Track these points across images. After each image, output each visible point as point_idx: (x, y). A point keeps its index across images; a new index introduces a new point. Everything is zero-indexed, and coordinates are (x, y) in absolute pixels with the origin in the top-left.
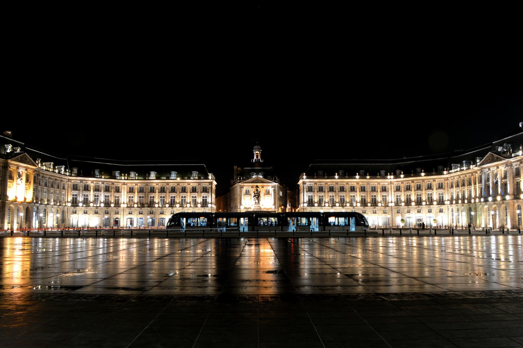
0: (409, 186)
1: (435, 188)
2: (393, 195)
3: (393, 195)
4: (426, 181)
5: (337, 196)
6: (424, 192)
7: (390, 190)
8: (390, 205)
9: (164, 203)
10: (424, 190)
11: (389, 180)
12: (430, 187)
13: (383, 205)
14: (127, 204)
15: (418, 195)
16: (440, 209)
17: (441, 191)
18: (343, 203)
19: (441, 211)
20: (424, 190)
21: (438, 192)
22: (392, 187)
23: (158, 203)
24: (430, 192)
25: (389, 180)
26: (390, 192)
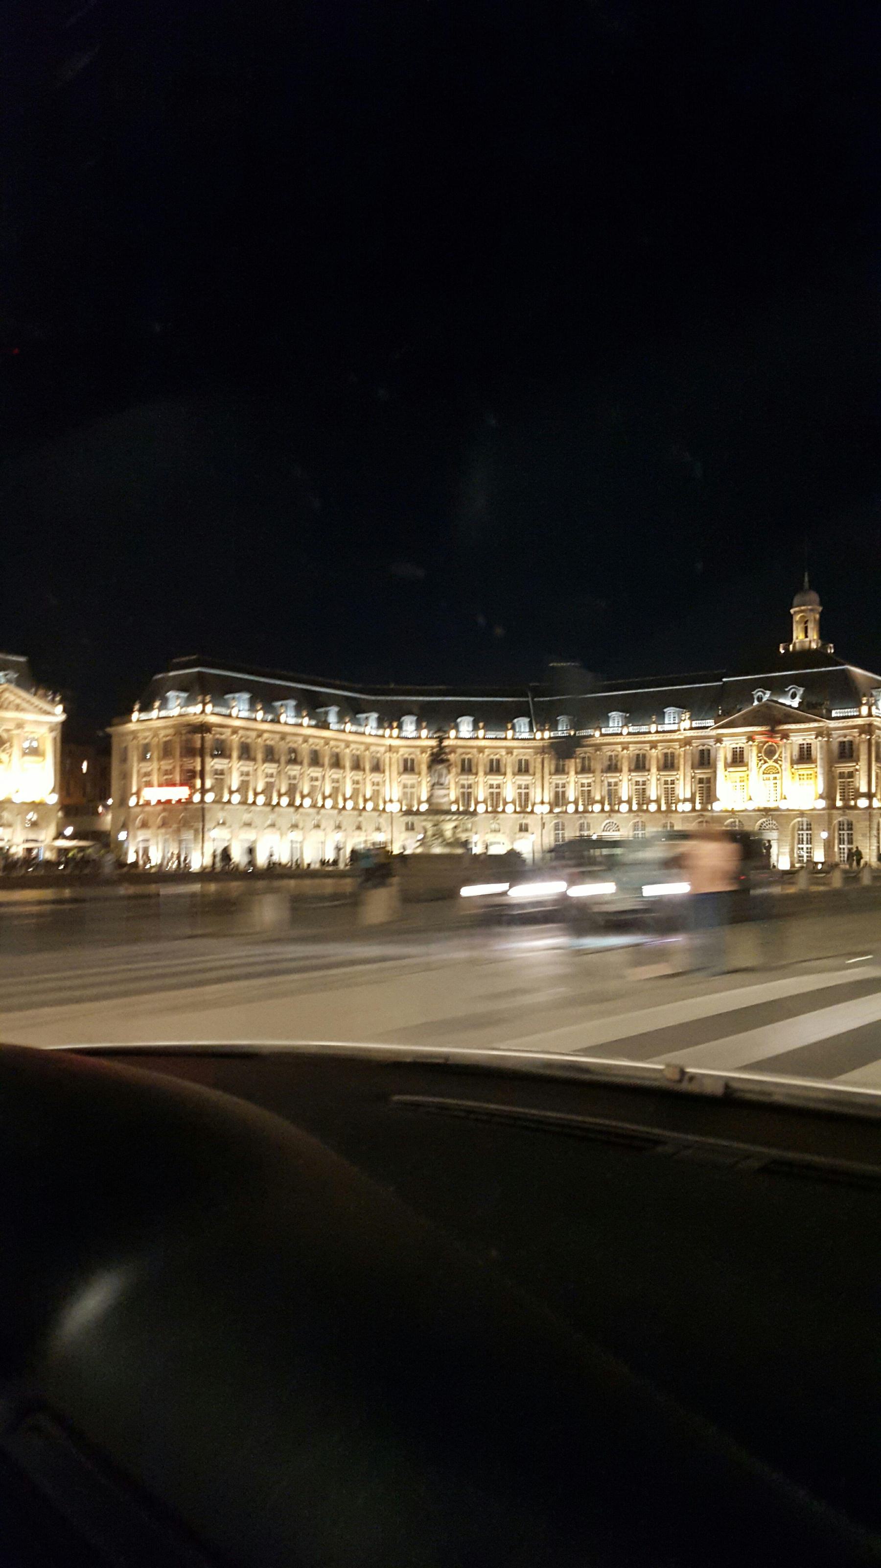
0: (498, 761)
1: (509, 771)
2: (395, 784)
3: (395, 784)
4: (487, 751)
5: (283, 776)
6: (481, 778)
7: (387, 768)
8: (389, 807)
9: (589, 800)
10: (481, 773)
11: (388, 742)
12: (495, 768)
13: (518, 809)
14: (549, 803)
15: (520, 787)
16: (521, 825)
17: (524, 780)
18: (526, 806)
19: (524, 829)
20: (481, 773)
21: (555, 782)
22: (393, 760)
23: (658, 801)
24: (495, 780)
25: (388, 742)
26: (387, 773)
